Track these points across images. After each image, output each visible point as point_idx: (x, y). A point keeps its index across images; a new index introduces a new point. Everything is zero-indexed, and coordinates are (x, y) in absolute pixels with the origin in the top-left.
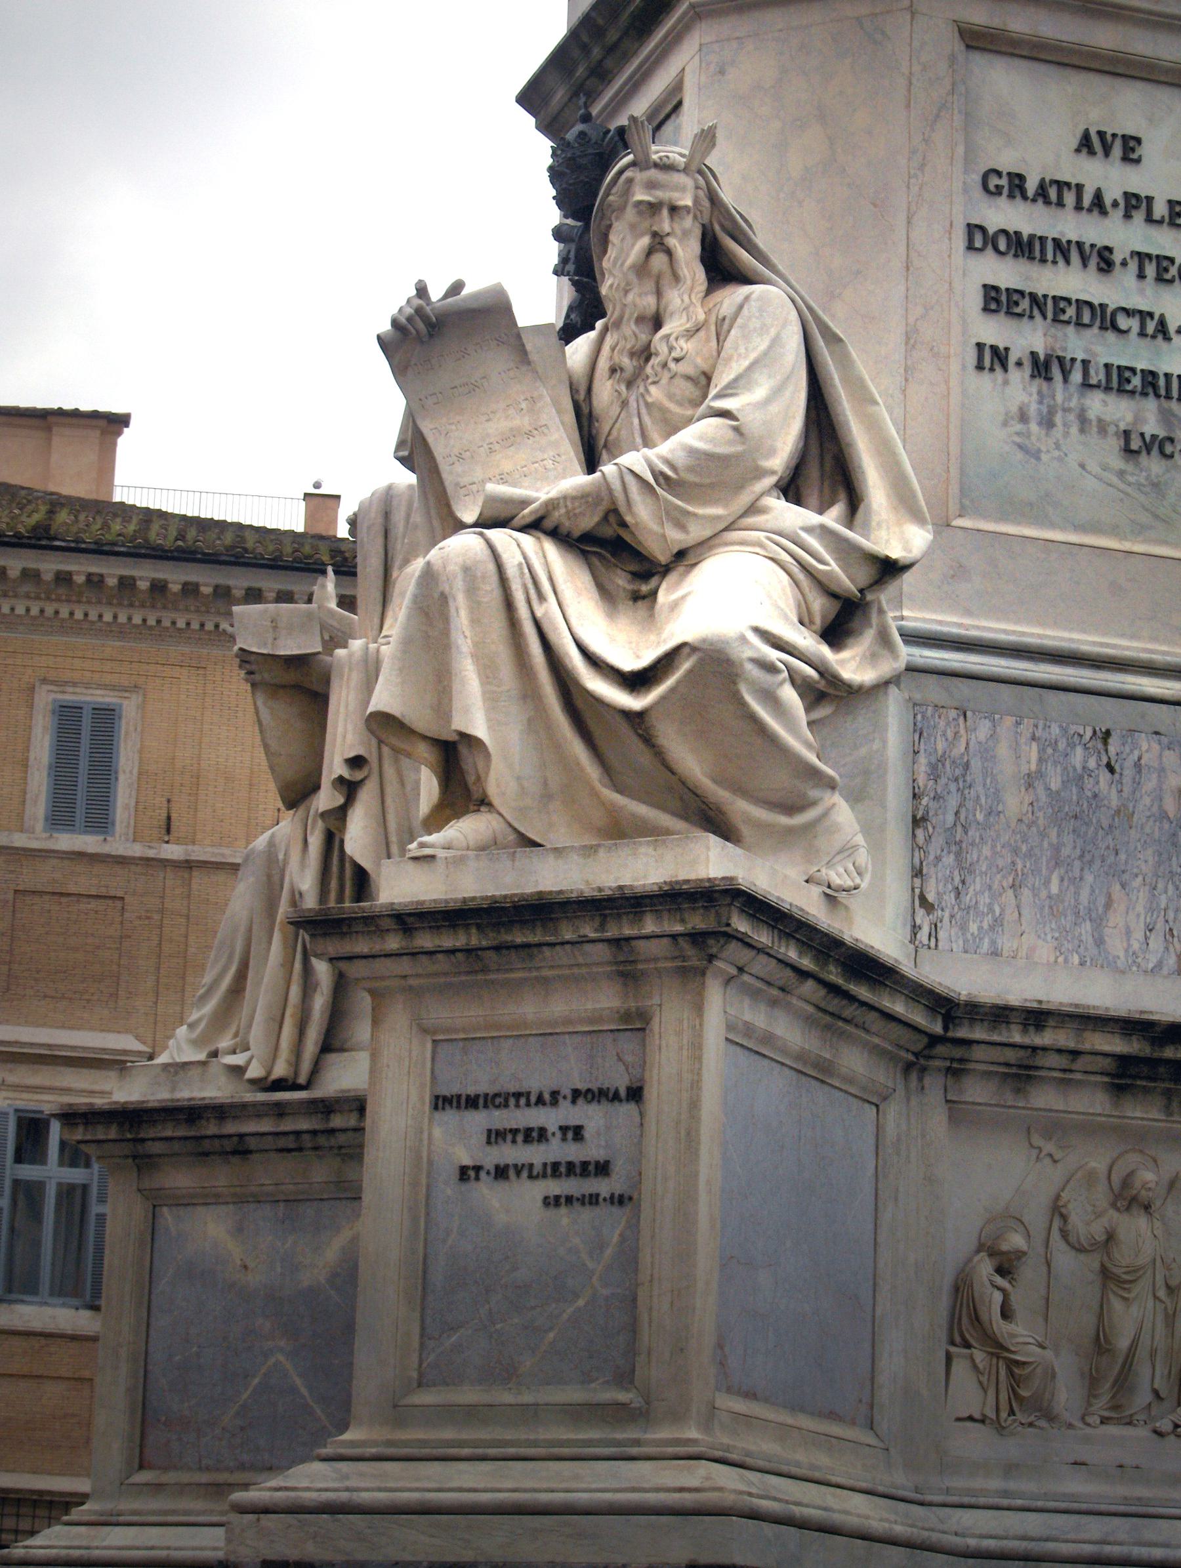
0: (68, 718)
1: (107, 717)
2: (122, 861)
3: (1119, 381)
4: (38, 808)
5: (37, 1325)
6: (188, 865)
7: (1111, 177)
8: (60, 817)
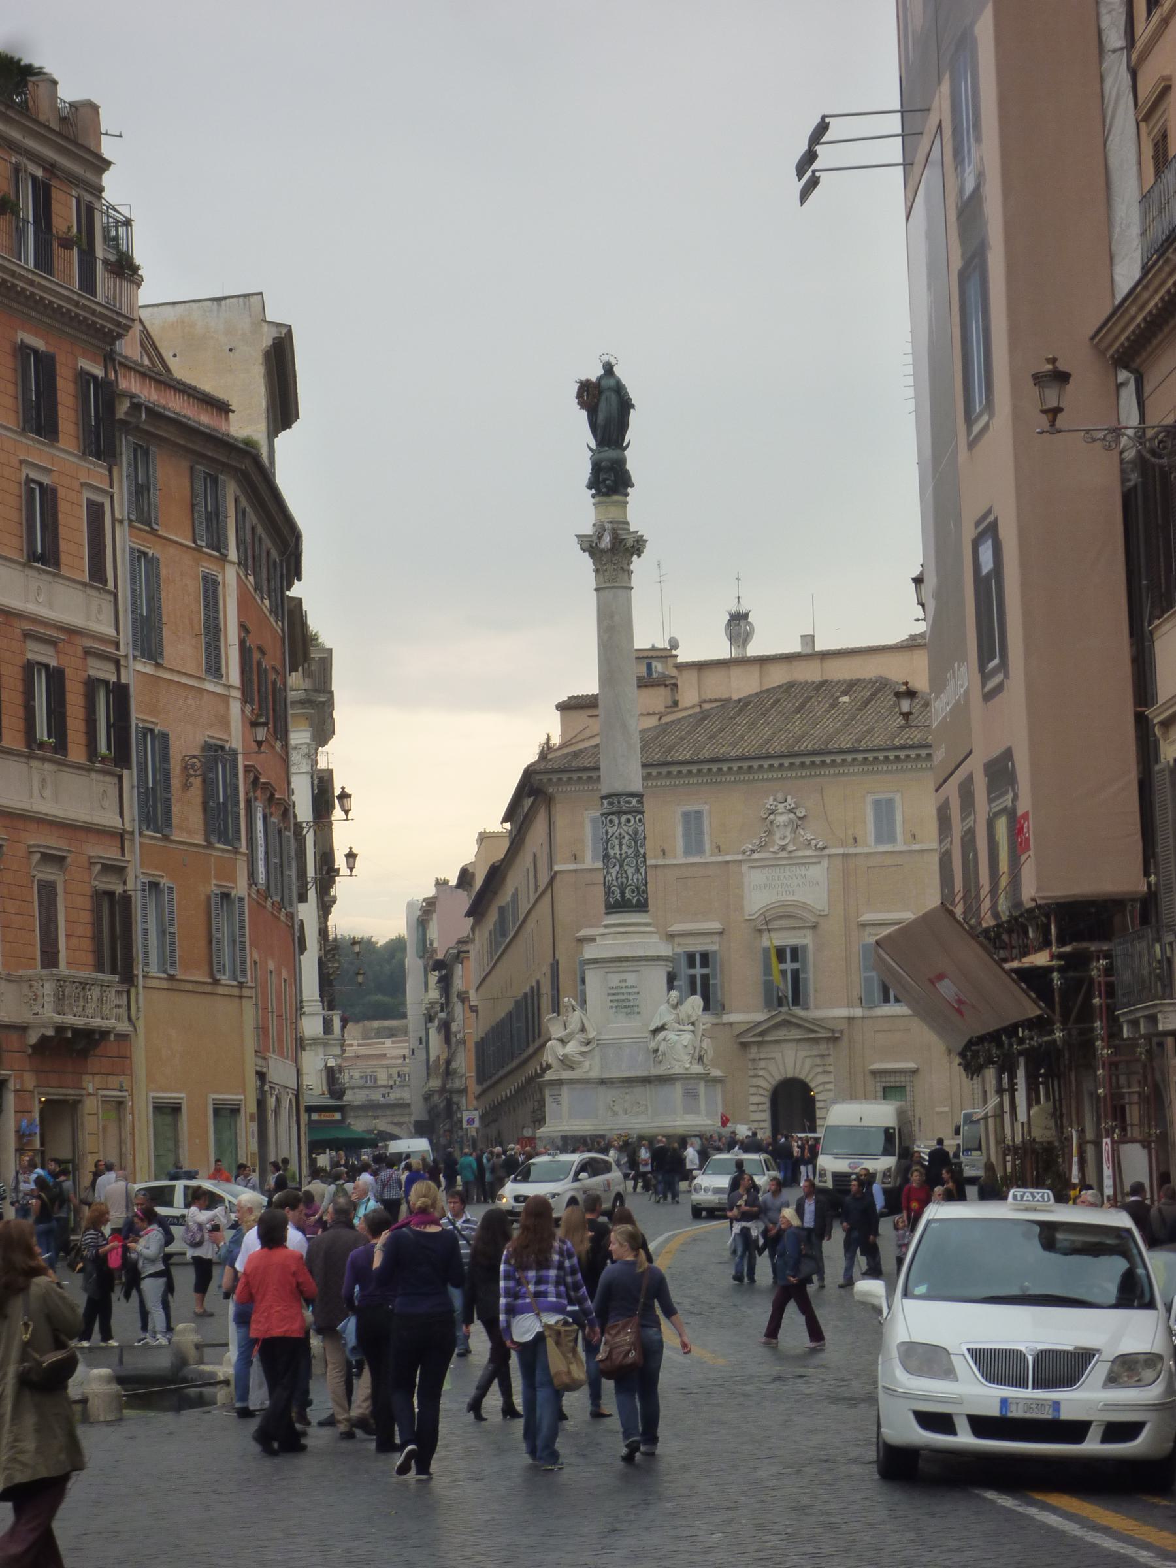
0: (877, 804)
1: (890, 802)
2: (901, 852)
3: (625, 1007)
4: (871, 838)
5: (889, 1013)
6: (922, 851)
7: (623, 984)
8: (879, 840)
